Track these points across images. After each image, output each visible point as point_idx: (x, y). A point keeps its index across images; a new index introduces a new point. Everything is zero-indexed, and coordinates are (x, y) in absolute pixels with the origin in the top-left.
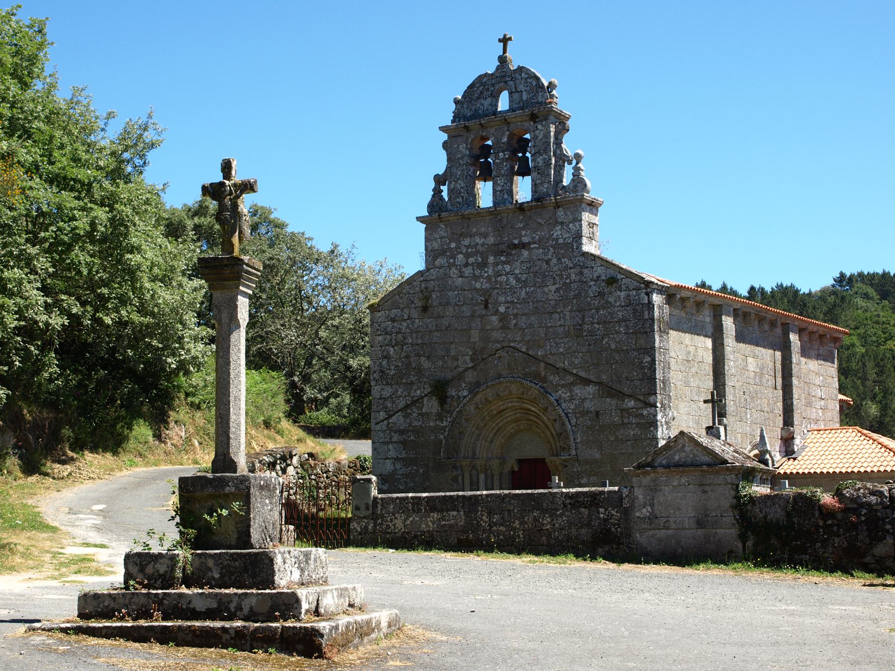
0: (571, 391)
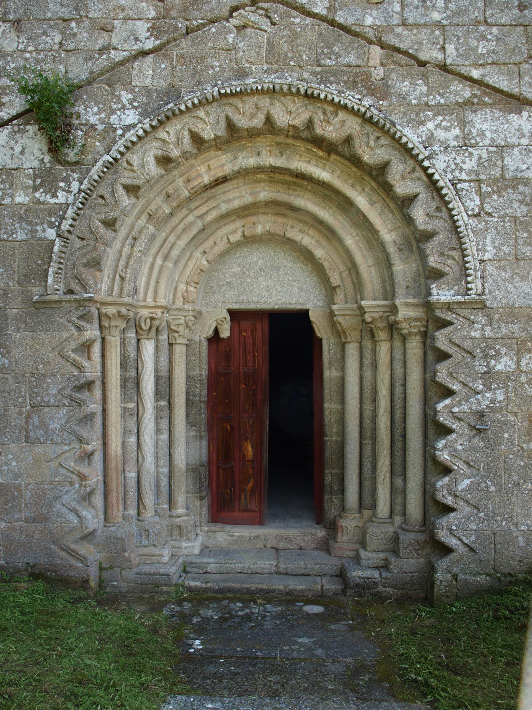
0: (463, 124)
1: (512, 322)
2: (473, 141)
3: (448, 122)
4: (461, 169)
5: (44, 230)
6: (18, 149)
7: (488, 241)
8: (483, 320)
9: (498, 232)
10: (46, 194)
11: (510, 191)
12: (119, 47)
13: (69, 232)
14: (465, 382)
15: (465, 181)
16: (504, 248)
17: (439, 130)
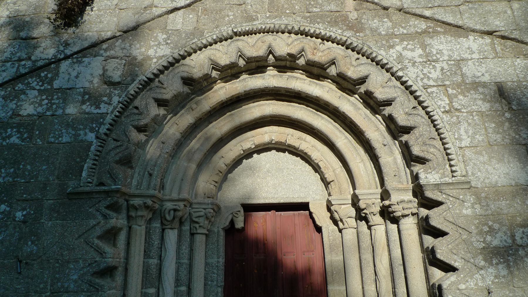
0: (424, 46)
1: (499, 200)
2: (435, 58)
3: (412, 45)
4: (429, 78)
5: (86, 134)
6: (74, 74)
7: (462, 132)
8: (472, 199)
9: (469, 124)
10: (91, 107)
11: (472, 92)
12: (159, 5)
13: (106, 134)
14: (466, 258)
15: (434, 86)
16: (477, 136)
17: (406, 51)
